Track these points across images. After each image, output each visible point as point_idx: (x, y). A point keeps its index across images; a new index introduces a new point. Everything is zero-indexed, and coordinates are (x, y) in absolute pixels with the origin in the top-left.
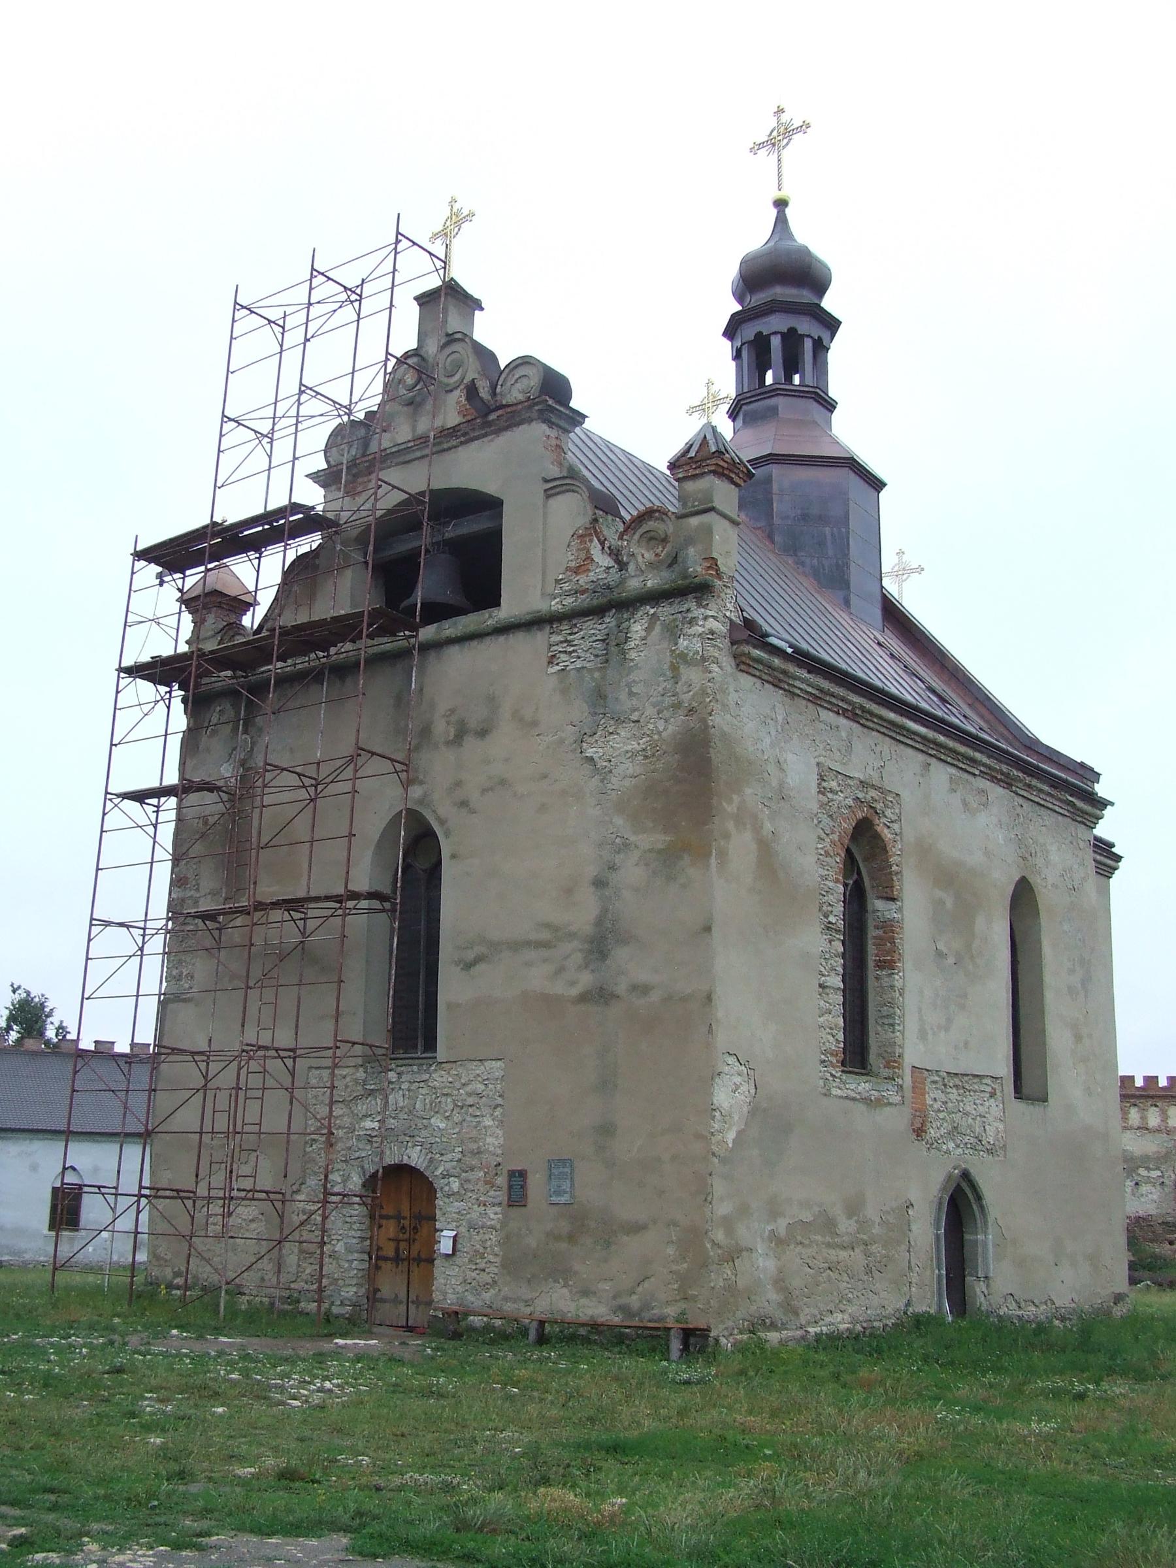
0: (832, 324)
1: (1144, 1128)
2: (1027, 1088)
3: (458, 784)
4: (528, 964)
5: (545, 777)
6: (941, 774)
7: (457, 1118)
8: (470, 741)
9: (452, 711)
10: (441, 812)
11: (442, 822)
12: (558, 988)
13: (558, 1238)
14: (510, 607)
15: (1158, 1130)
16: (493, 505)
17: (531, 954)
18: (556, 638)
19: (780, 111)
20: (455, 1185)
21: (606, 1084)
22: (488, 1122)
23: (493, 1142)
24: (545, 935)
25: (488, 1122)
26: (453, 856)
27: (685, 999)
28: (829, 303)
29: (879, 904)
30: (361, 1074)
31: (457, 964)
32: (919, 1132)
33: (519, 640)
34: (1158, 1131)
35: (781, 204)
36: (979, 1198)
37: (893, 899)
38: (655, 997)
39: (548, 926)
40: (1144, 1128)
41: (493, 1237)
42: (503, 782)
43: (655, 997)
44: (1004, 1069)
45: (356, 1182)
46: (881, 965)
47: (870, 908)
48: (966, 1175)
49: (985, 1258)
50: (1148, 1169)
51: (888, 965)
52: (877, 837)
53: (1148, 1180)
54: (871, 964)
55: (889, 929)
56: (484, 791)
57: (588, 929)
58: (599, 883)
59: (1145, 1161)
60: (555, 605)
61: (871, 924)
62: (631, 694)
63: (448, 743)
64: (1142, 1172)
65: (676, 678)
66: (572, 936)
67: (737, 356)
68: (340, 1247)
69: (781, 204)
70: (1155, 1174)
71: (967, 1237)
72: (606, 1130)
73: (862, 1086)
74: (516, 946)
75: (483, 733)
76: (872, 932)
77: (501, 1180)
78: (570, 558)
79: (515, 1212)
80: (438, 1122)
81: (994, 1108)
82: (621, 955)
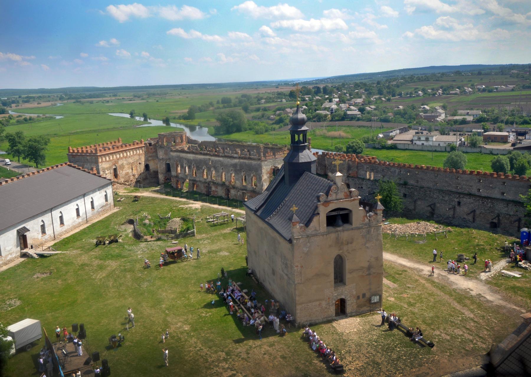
1: (106, 161)
3: (348, 250)
11: (346, 255)
15: (109, 161)
16: (351, 211)
20: (349, 299)
23: (355, 293)
26: (348, 260)
34: (109, 161)
40: (106, 161)
41: (355, 304)
45: (334, 302)
58: (368, 261)
59: (108, 169)
72: (370, 289)
75: (351, 243)
78: (362, 219)
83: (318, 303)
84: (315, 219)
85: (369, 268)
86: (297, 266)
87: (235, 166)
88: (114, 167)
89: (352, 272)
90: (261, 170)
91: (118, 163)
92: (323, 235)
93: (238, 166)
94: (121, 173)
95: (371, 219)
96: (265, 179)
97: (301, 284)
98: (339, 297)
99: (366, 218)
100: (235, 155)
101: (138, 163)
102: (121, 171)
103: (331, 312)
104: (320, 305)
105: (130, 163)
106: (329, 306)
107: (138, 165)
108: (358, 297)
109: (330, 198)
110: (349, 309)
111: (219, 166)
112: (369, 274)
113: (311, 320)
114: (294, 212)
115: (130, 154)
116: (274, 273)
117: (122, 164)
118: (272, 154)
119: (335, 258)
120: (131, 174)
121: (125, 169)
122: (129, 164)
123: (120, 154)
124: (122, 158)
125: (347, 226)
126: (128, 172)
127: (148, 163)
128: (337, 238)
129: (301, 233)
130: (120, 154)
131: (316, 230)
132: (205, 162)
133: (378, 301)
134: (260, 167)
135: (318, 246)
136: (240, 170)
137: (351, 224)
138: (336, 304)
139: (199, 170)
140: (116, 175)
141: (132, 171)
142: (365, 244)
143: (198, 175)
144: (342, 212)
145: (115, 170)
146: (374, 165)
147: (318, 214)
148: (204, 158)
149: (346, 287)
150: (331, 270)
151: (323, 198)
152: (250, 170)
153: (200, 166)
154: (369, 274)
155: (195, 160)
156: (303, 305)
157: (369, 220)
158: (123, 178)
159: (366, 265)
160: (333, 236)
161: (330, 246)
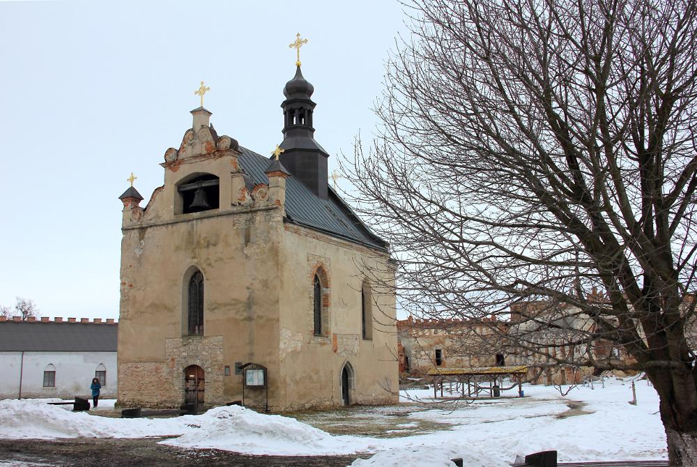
0: (314, 105)
2: (367, 335)
3: (208, 259)
4: (229, 310)
5: (232, 258)
6: (342, 250)
7: (210, 352)
8: (211, 247)
9: (207, 237)
11: (203, 269)
12: (238, 316)
16: (217, 178)
18: (235, 219)
19: (298, 35)
20: (210, 370)
21: (251, 343)
22: (218, 353)
23: (220, 358)
24: (233, 302)
25: (218, 353)
27: (272, 320)
28: (313, 98)
29: (324, 289)
30: (181, 340)
31: (209, 309)
32: (335, 351)
33: (224, 219)
35: (299, 67)
36: (352, 368)
37: (327, 288)
38: (264, 319)
41: (220, 384)
42: (221, 259)
43: (264, 319)
44: (359, 331)
45: (181, 370)
46: (324, 306)
47: (321, 290)
48: (348, 362)
49: (354, 385)
51: (327, 306)
52: (323, 271)
54: (322, 305)
55: (327, 297)
56: (216, 261)
57: (245, 300)
58: (248, 288)
61: (322, 295)
62: (257, 237)
63: (205, 247)
65: (269, 233)
66: (241, 302)
67: (285, 113)
68: (177, 388)
69: (299, 67)
71: (349, 378)
72: (252, 354)
73: (320, 339)
74: (225, 305)
75: (215, 245)
76: (322, 297)
77: (223, 368)
78: (239, 196)
81: (357, 343)
82: (255, 308)
83: (152, 366)
85: (250, 303)
97: (126, 319)
98: (191, 363)
103: (175, 390)
104: (157, 369)
112: (250, 319)
128: (190, 234)
129: (135, 221)
133: (261, 383)
135: (158, 246)
144: (205, 184)
145: (438, 353)
149: (205, 341)
150: (178, 298)
154: (250, 319)
156: (130, 365)
159: (243, 296)
160: (183, 227)
161: (178, 248)
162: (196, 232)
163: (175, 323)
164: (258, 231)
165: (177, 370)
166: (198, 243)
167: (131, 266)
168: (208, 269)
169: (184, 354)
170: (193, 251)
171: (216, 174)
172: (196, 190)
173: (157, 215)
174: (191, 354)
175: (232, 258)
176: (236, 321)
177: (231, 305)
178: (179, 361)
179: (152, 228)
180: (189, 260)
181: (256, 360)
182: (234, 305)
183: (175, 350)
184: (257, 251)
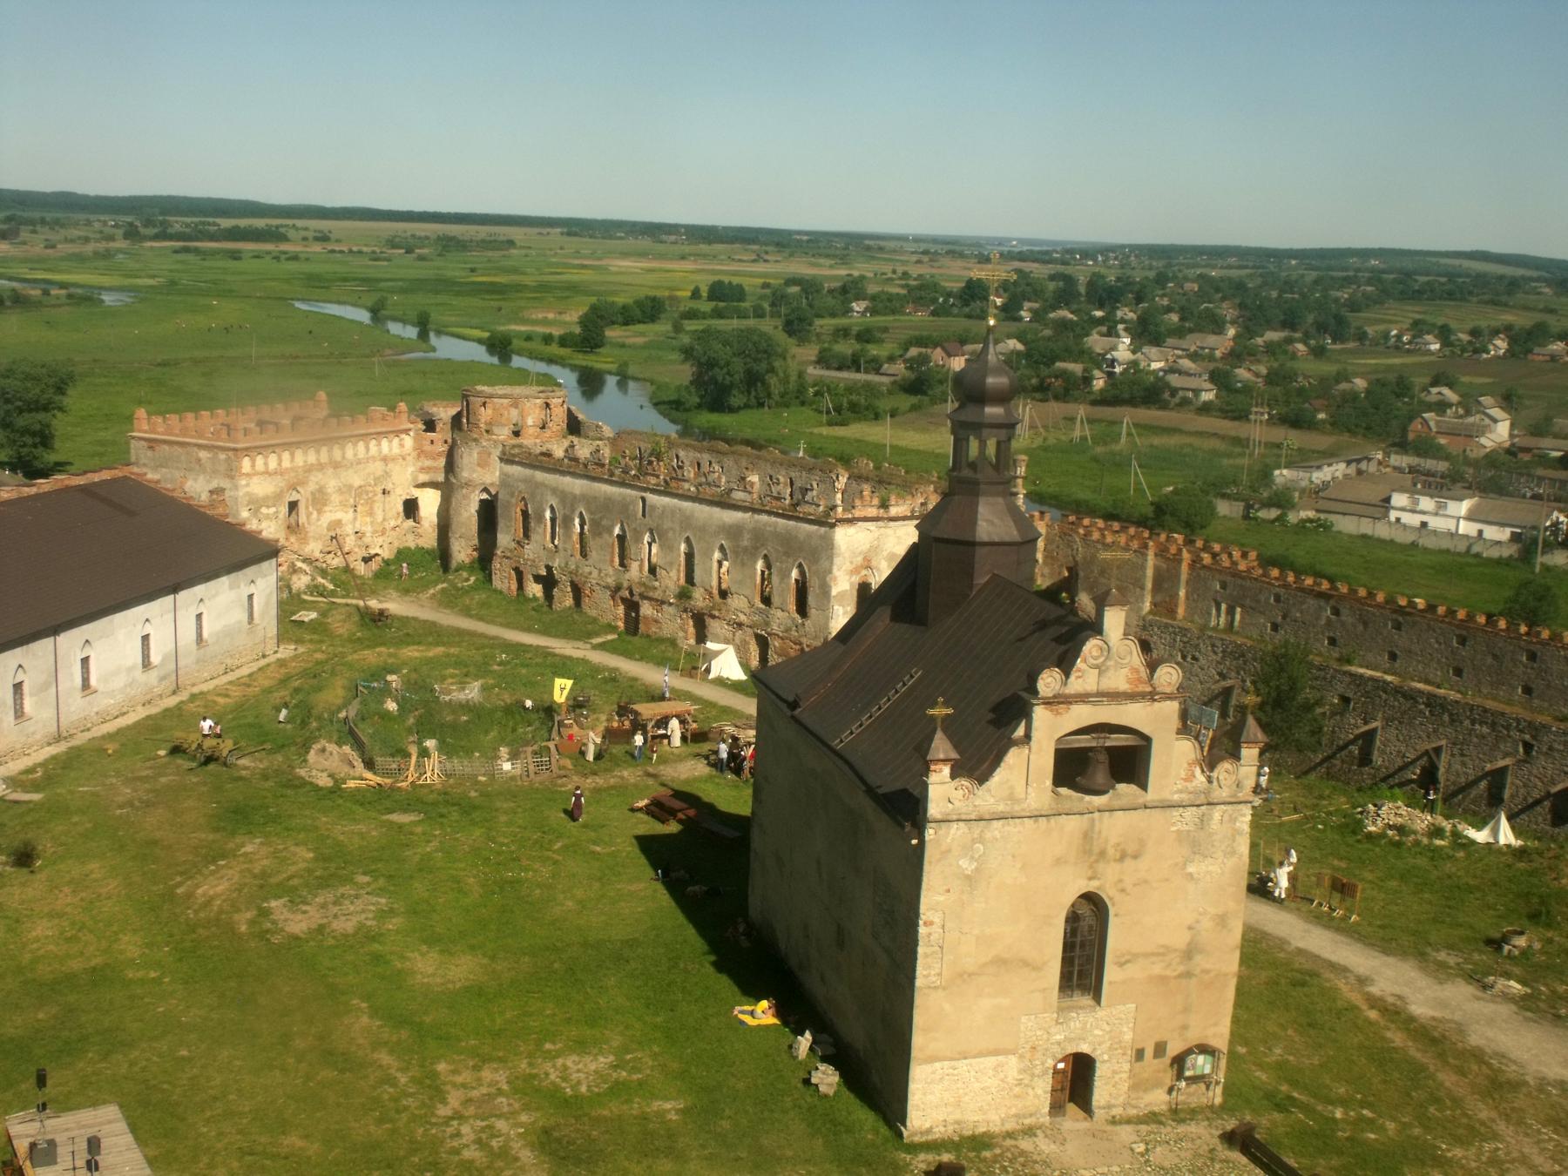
3: (1120, 881)
4: (1153, 963)
5: (1167, 880)
7: (1108, 1028)
9: (1118, 844)
10: (1111, 894)
11: (1111, 899)
12: (1168, 973)
13: (1159, 1072)
14: (1152, 795)
16: (1147, 740)
17: (1154, 959)
20: (1106, 1057)
21: (1186, 1010)
22: (1125, 1029)
23: (1128, 1037)
24: (1161, 950)
25: (1125, 1029)
27: (1226, 975)
38: (1212, 974)
39: (1163, 946)
40: (262, 473)
41: (1125, 1076)
42: (1146, 882)
43: (1212, 974)
45: (1050, 1063)
50: (268, 507)
53: (267, 517)
56: (1135, 885)
58: (1190, 928)
60: (1176, 797)
63: (1115, 860)
64: (264, 510)
66: (1176, 950)
68: (1040, 1092)
70: (273, 510)
72: (1185, 1027)
74: (1146, 955)
75: (1135, 857)
79: (1139, 1064)
80: (1097, 1032)
82: (1198, 958)
83: (991, 1061)
84: (1013, 757)
85: (1189, 953)
86: (931, 923)
87: (734, 532)
88: (294, 497)
89: (1128, 962)
90: (831, 558)
91: (303, 483)
92: (1035, 817)
93: (747, 536)
94: (317, 523)
95: (1214, 774)
96: (842, 595)
99: (1198, 771)
100: (738, 495)
101: (379, 490)
102: (315, 514)
104: (997, 1068)
105: (350, 487)
106: (1033, 1075)
107: (380, 495)
108: (1140, 1054)
109: (1076, 685)
110: (1102, 1093)
111: (678, 528)
112: (1188, 975)
113: (958, 1122)
114: (939, 723)
115: (355, 455)
116: (841, 938)
117: (321, 490)
118: (876, 501)
119: (1073, 905)
120: (349, 529)
121: (326, 508)
122: (346, 489)
123: (318, 452)
124: (321, 467)
125: (1126, 791)
126: (338, 523)
127: (417, 493)
128: (1087, 836)
130: (318, 452)
131: (1011, 798)
132: (624, 509)
134: (828, 546)
135: (1013, 856)
136: (752, 553)
137: (1143, 786)
138: (1056, 1071)
139: (600, 534)
140: (293, 528)
141: (355, 519)
142: (1185, 864)
143: (594, 555)
145: (293, 506)
146: (1248, 583)
147: (1028, 737)
148: (620, 494)
149: (1101, 1013)
151: (1048, 682)
152: (787, 554)
153: (604, 522)
154: (1188, 975)
155: (588, 499)
156: (938, 1065)
157: (1210, 781)
158: (316, 539)
159: (1181, 940)
160: (1073, 824)
161: (1058, 861)
162: (1100, 832)
163: (1044, 990)
164: (1215, 837)
165: (1043, 1064)
166: (1102, 854)
167: (948, 891)
168: (1118, 897)
169: (1058, 1037)
170: (1091, 867)
171: (1146, 730)
172: (1091, 749)
173: (1012, 794)
174: (1073, 1035)
175: (1167, 880)
176: (1163, 979)
177: (1158, 954)
178: (1047, 1050)
179: (1001, 822)
180: (1086, 882)
181: (1194, 1037)
182: (1163, 954)
183: (1039, 1033)
184: (1211, 868)
